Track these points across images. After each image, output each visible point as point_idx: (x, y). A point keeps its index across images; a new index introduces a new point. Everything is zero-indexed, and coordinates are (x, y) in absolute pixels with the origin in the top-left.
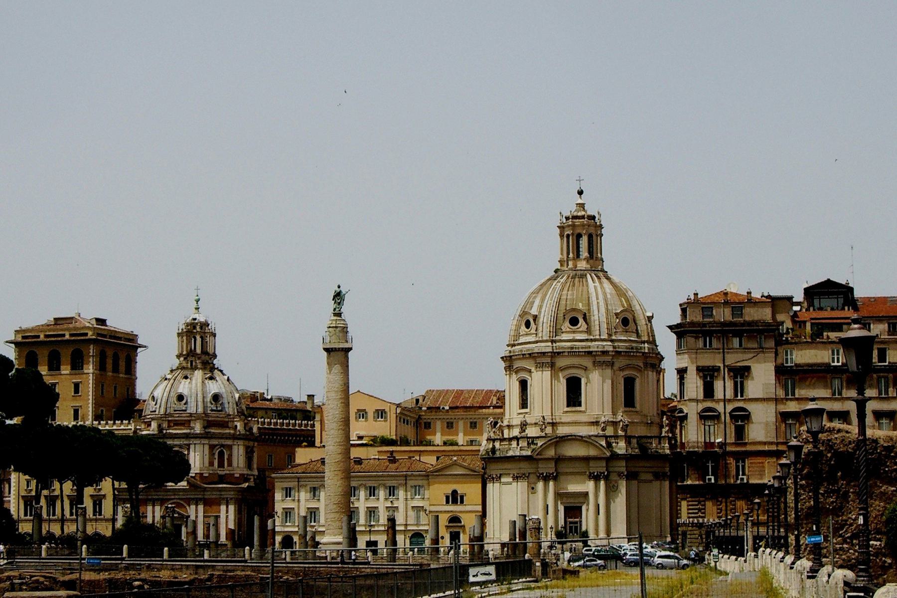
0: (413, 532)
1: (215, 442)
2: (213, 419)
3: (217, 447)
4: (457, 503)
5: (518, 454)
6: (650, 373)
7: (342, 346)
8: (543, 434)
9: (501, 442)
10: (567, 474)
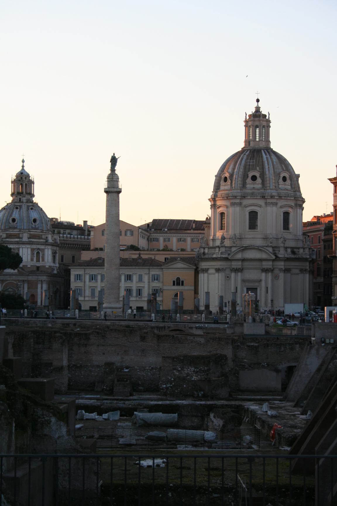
2: (33, 233)
4: (179, 285)
5: (219, 256)
6: (298, 210)
7: (115, 190)
8: (235, 245)
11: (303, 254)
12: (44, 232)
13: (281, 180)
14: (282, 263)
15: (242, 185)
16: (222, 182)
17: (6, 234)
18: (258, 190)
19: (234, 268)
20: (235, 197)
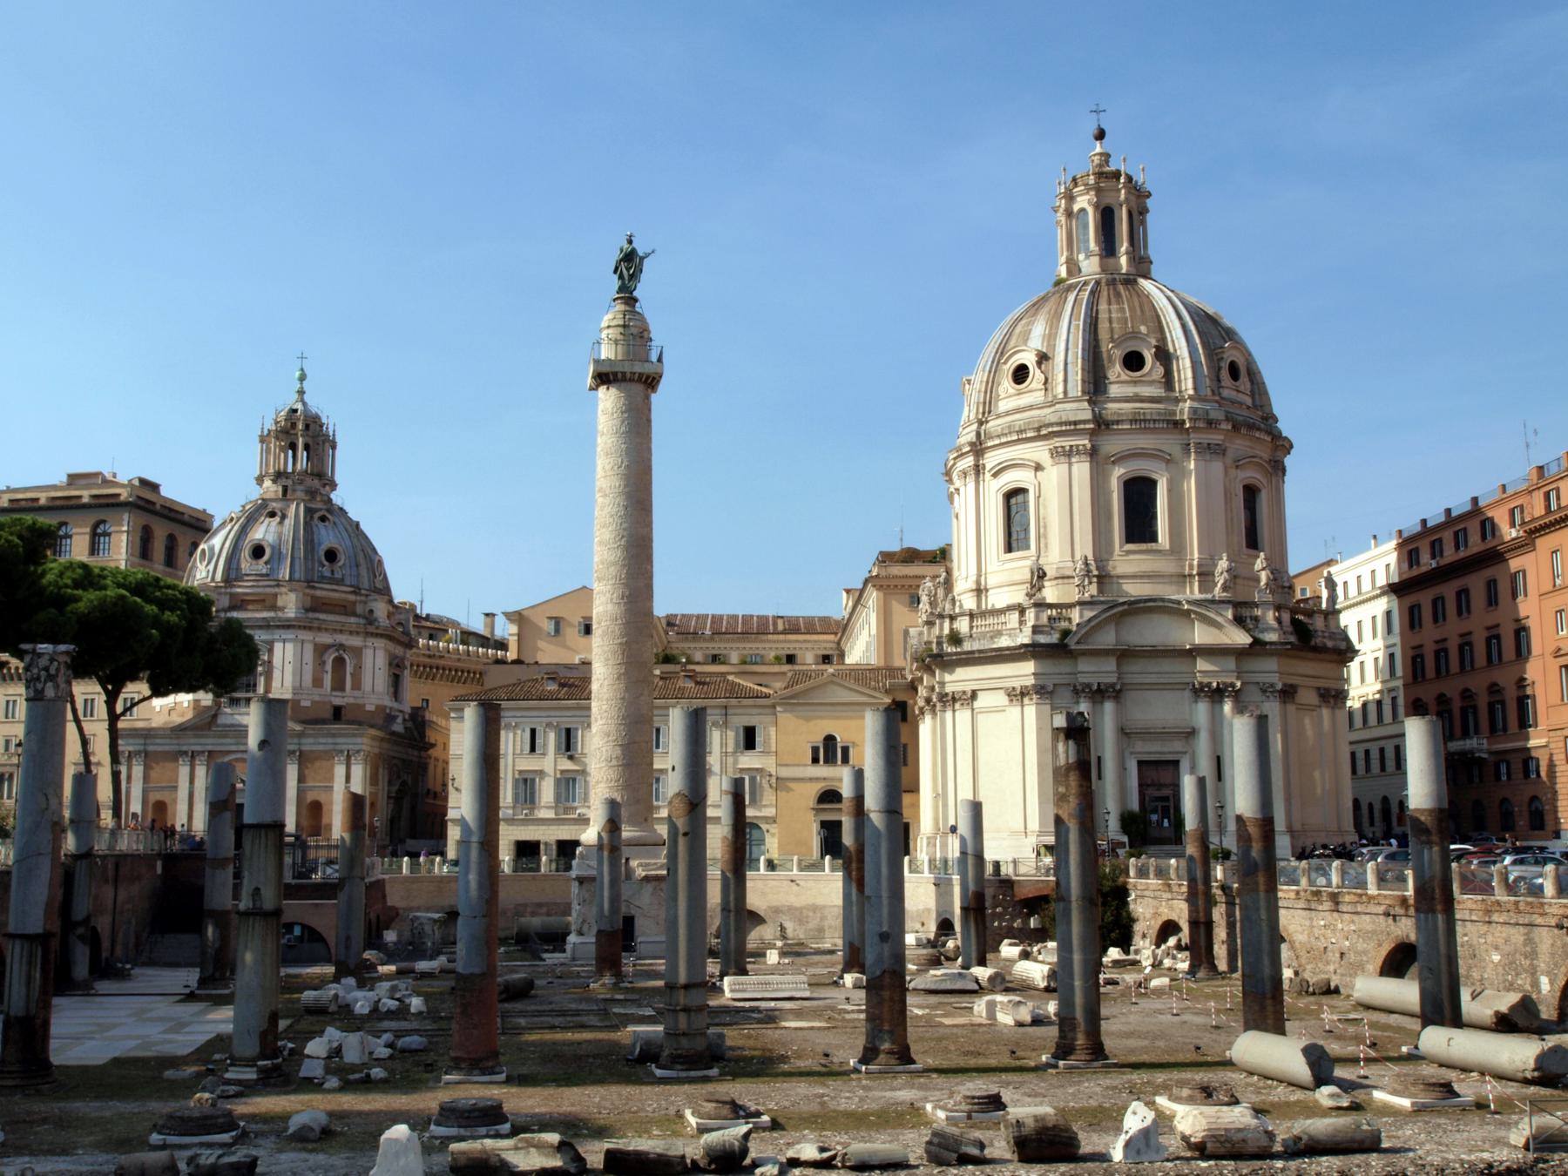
1: (326, 639)
3: (331, 650)
5: (1026, 641)
7: (638, 368)
10: (1143, 687)
11: (1326, 634)
12: (361, 595)
13: (1225, 374)
14: (1271, 664)
15: (1091, 385)
16: (1006, 384)
17: (232, 596)
19: (1089, 685)
20: (1071, 429)
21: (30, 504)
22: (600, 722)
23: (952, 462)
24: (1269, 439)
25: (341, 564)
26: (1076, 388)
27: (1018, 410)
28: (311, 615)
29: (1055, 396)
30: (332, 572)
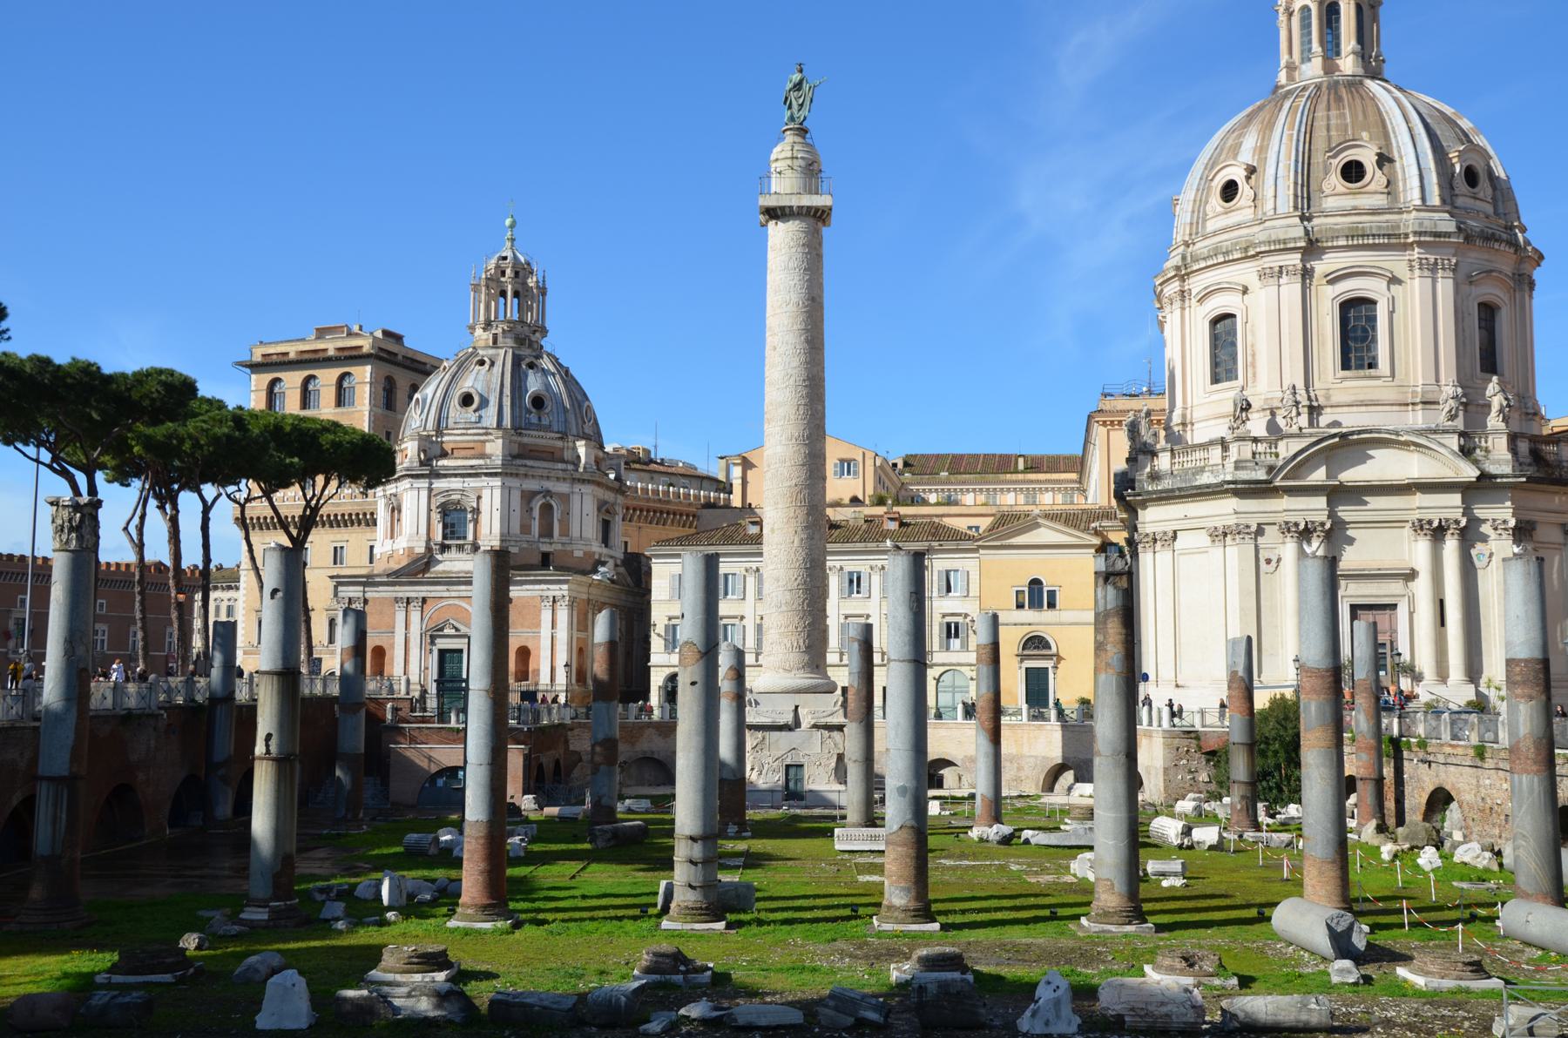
0: (943, 669)
1: (532, 485)
3: (538, 497)
4: (1040, 606)
5: (1229, 478)
9: (1173, 456)
16: (1215, 201)
18: (1374, 212)
21: (281, 359)
22: (771, 567)
23: (1159, 288)
24: (1512, 250)
25: (547, 411)
26: (1286, 203)
27: (1225, 230)
28: (519, 462)
29: (1264, 214)
30: (540, 419)
